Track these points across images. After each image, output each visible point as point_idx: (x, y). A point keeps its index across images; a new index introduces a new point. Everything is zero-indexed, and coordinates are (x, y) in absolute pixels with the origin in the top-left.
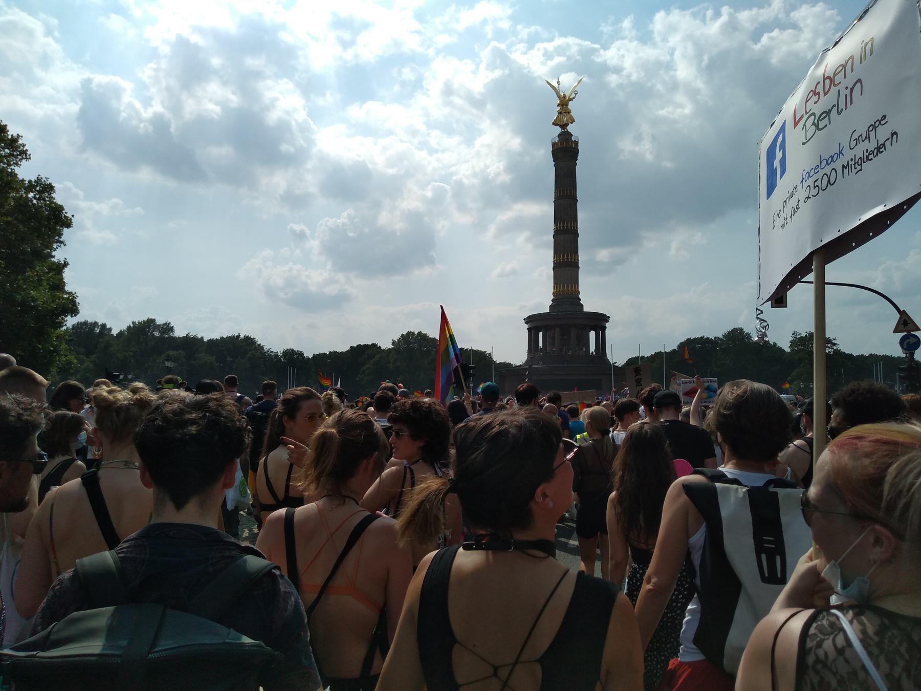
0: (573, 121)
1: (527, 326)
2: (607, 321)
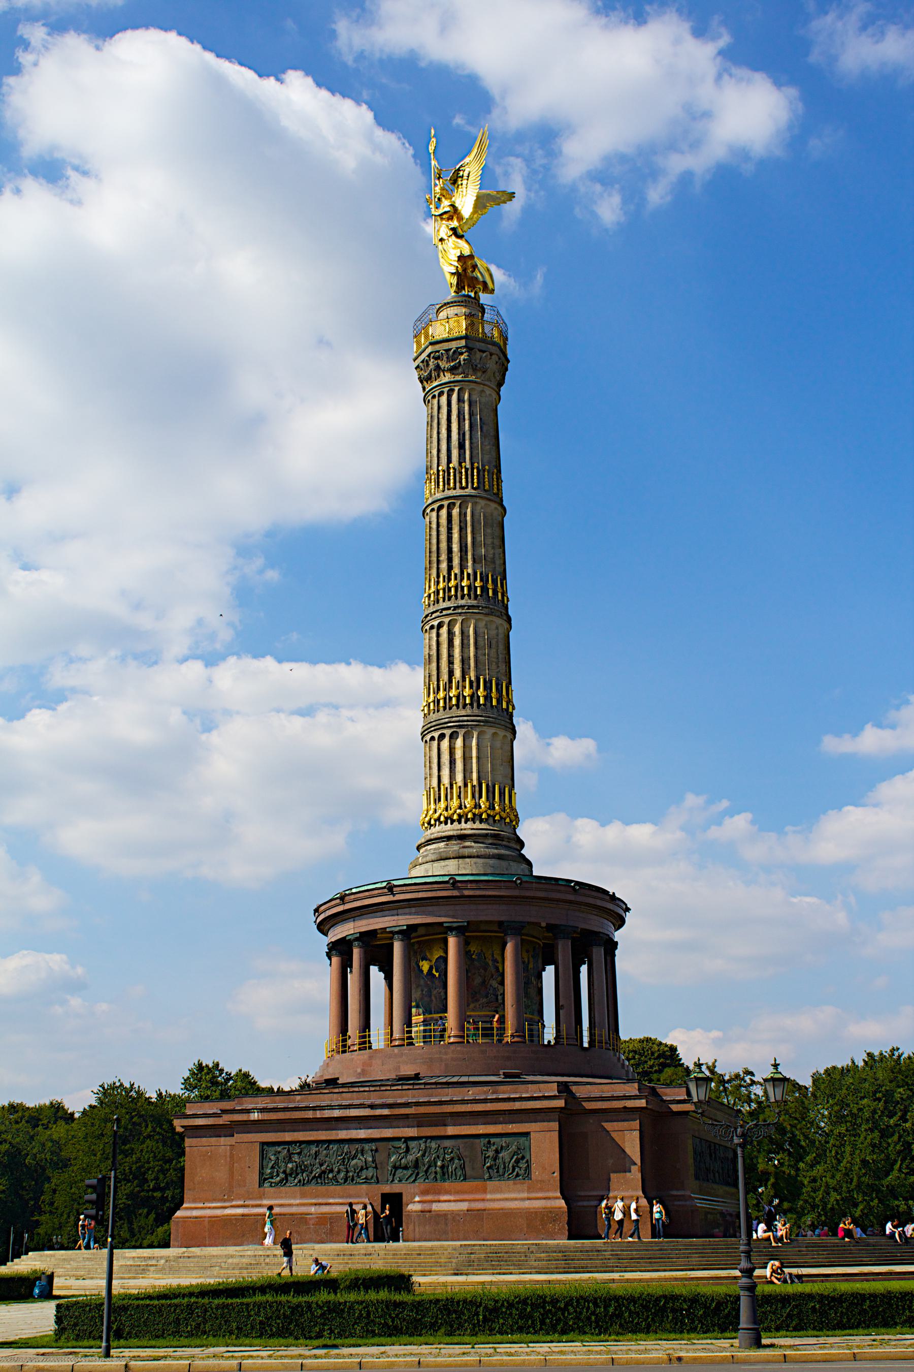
2: (620, 922)
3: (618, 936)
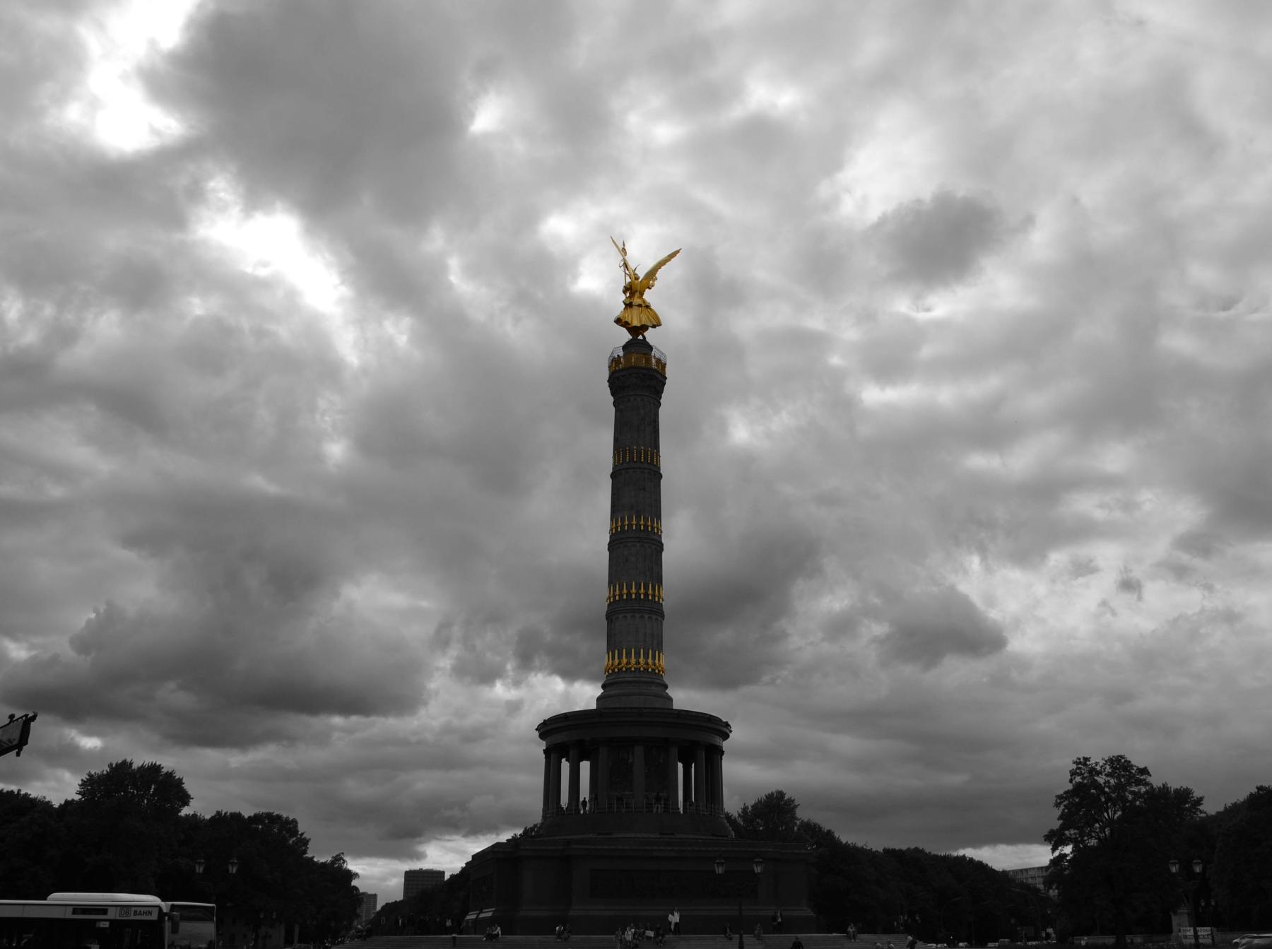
0: (657, 324)
1: (543, 745)
2: (726, 736)
3: (726, 745)
